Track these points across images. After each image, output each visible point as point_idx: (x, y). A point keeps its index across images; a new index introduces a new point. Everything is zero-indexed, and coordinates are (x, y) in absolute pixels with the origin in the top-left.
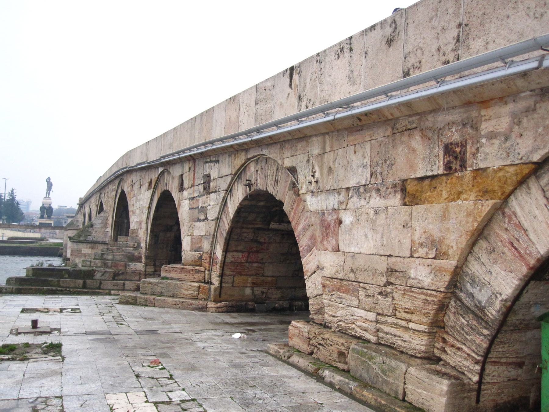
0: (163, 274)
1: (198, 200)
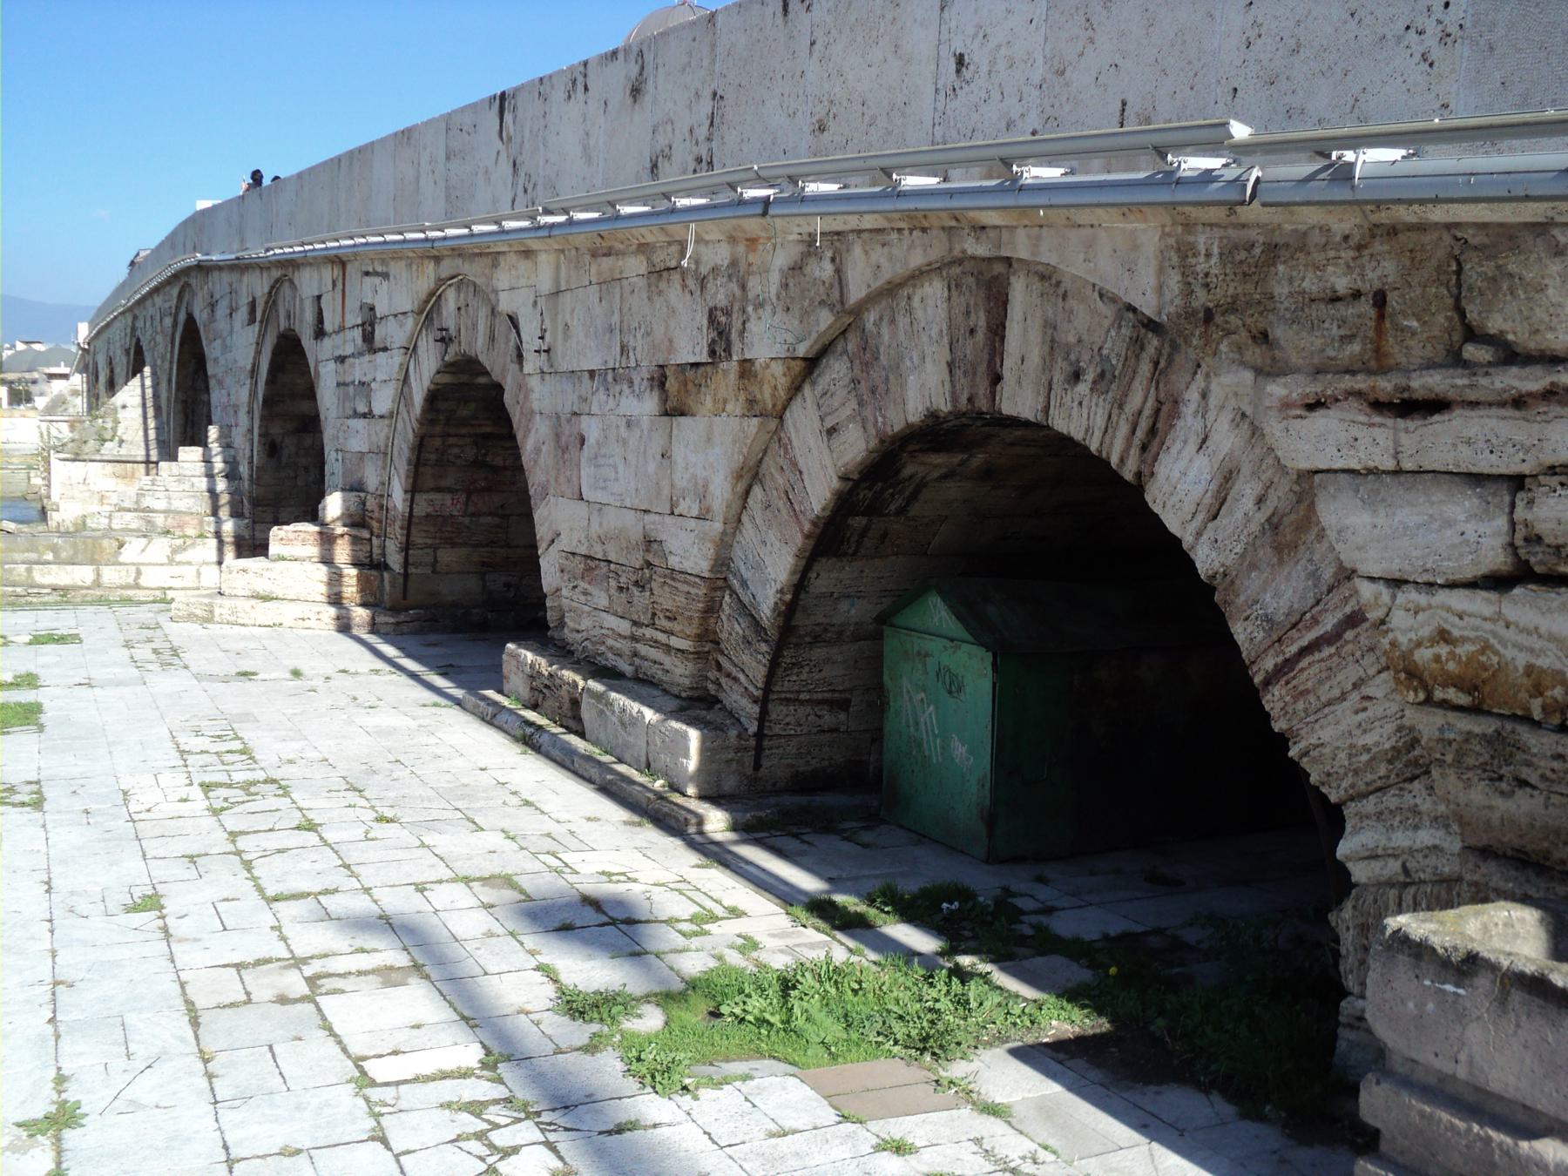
0: (274, 548)
1: (352, 366)
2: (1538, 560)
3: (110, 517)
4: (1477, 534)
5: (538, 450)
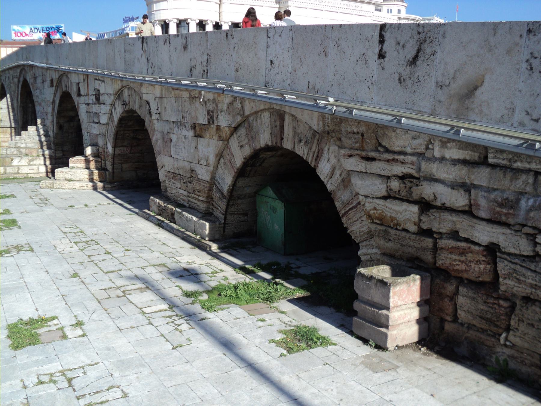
0: (71, 165)
1: (92, 107)
2: (392, 194)
3: (6, 150)
4: (380, 188)
5: (157, 141)
